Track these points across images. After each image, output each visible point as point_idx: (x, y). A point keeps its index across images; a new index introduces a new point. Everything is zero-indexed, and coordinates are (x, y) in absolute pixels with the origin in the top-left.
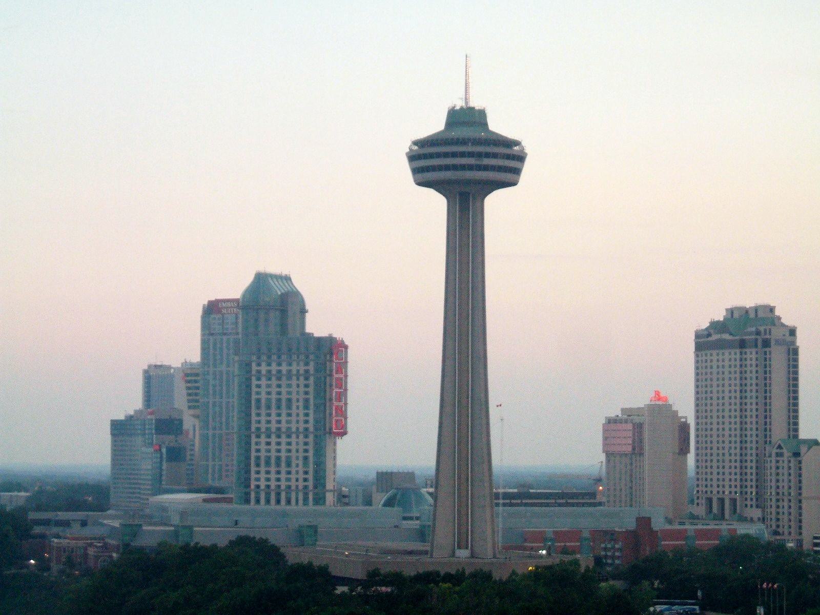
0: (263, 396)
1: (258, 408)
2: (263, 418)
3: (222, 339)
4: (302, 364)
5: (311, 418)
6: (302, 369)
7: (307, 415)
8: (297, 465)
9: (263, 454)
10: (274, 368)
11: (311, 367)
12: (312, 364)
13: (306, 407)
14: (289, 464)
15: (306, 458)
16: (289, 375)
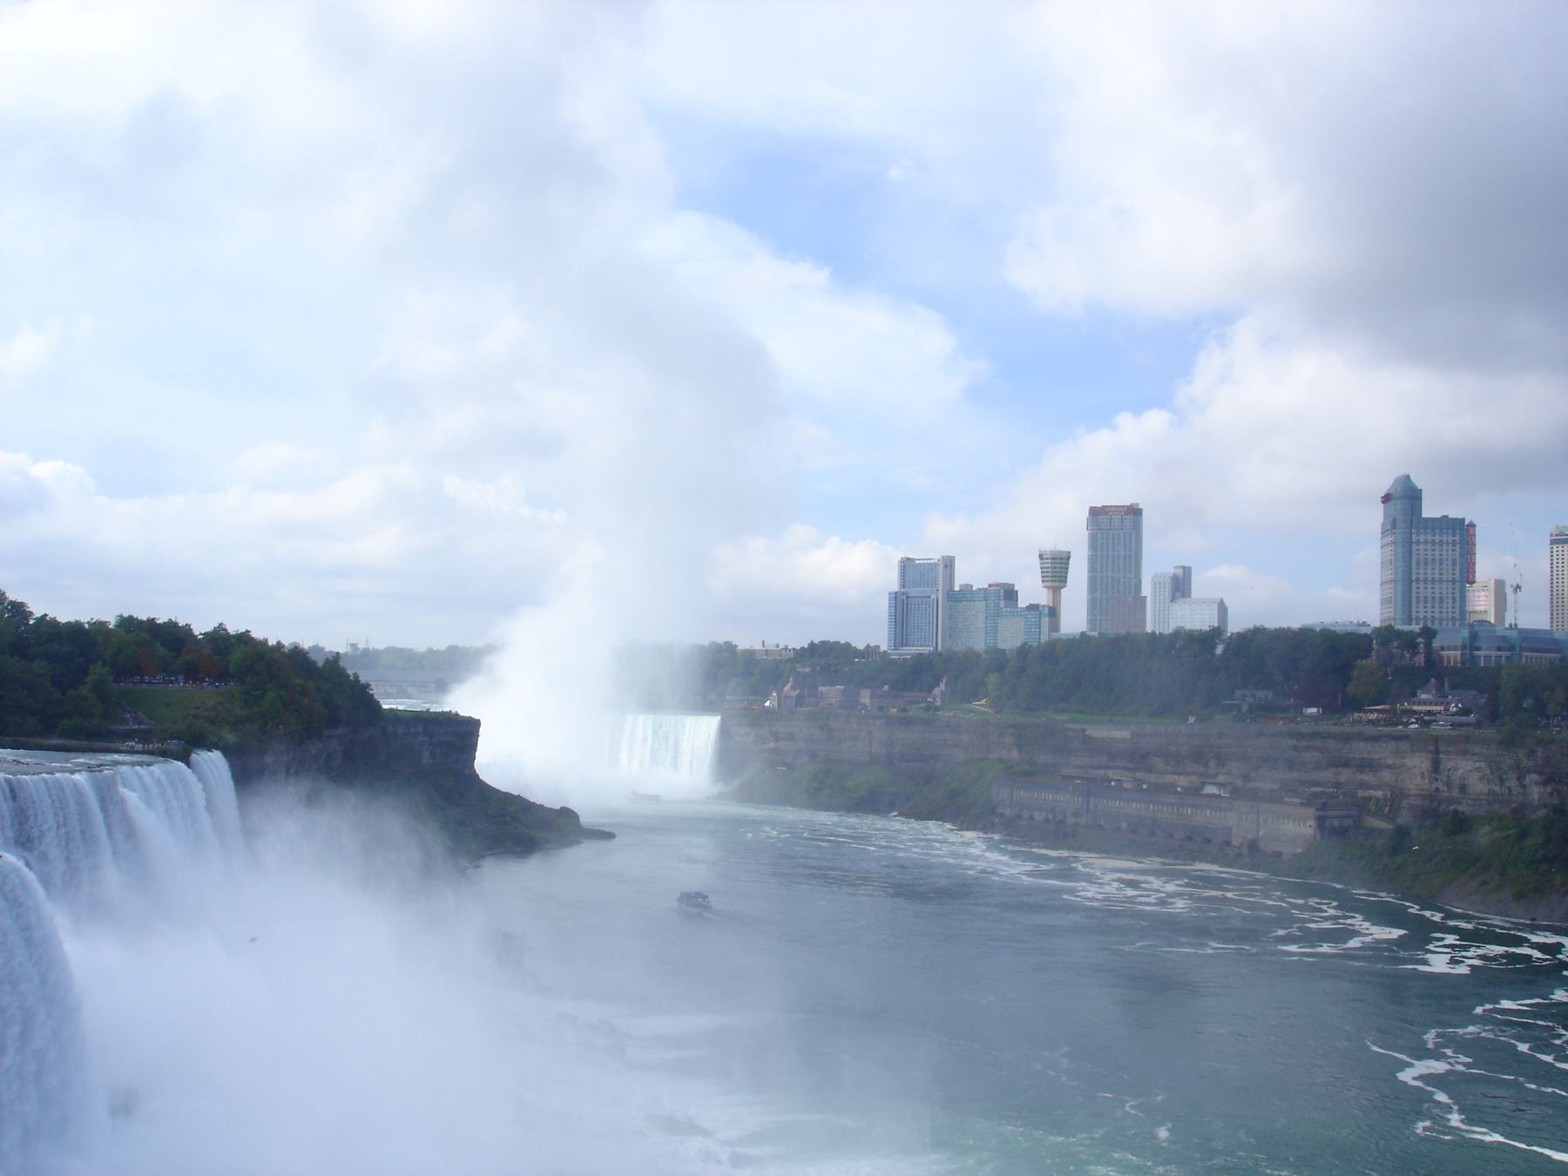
0: (1422, 557)
1: (1418, 564)
2: (1422, 571)
3: (1108, 535)
4: (1450, 536)
5: (1458, 574)
6: (1450, 539)
7: (1453, 569)
8: (1447, 603)
9: (1422, 595)
10: (1430, 538)
11: (1457, 538)
12: (1458, 536)
13: (1454, 565)
14: (1441, 602)
15: (1453, 598)
16: (1441, 543)
